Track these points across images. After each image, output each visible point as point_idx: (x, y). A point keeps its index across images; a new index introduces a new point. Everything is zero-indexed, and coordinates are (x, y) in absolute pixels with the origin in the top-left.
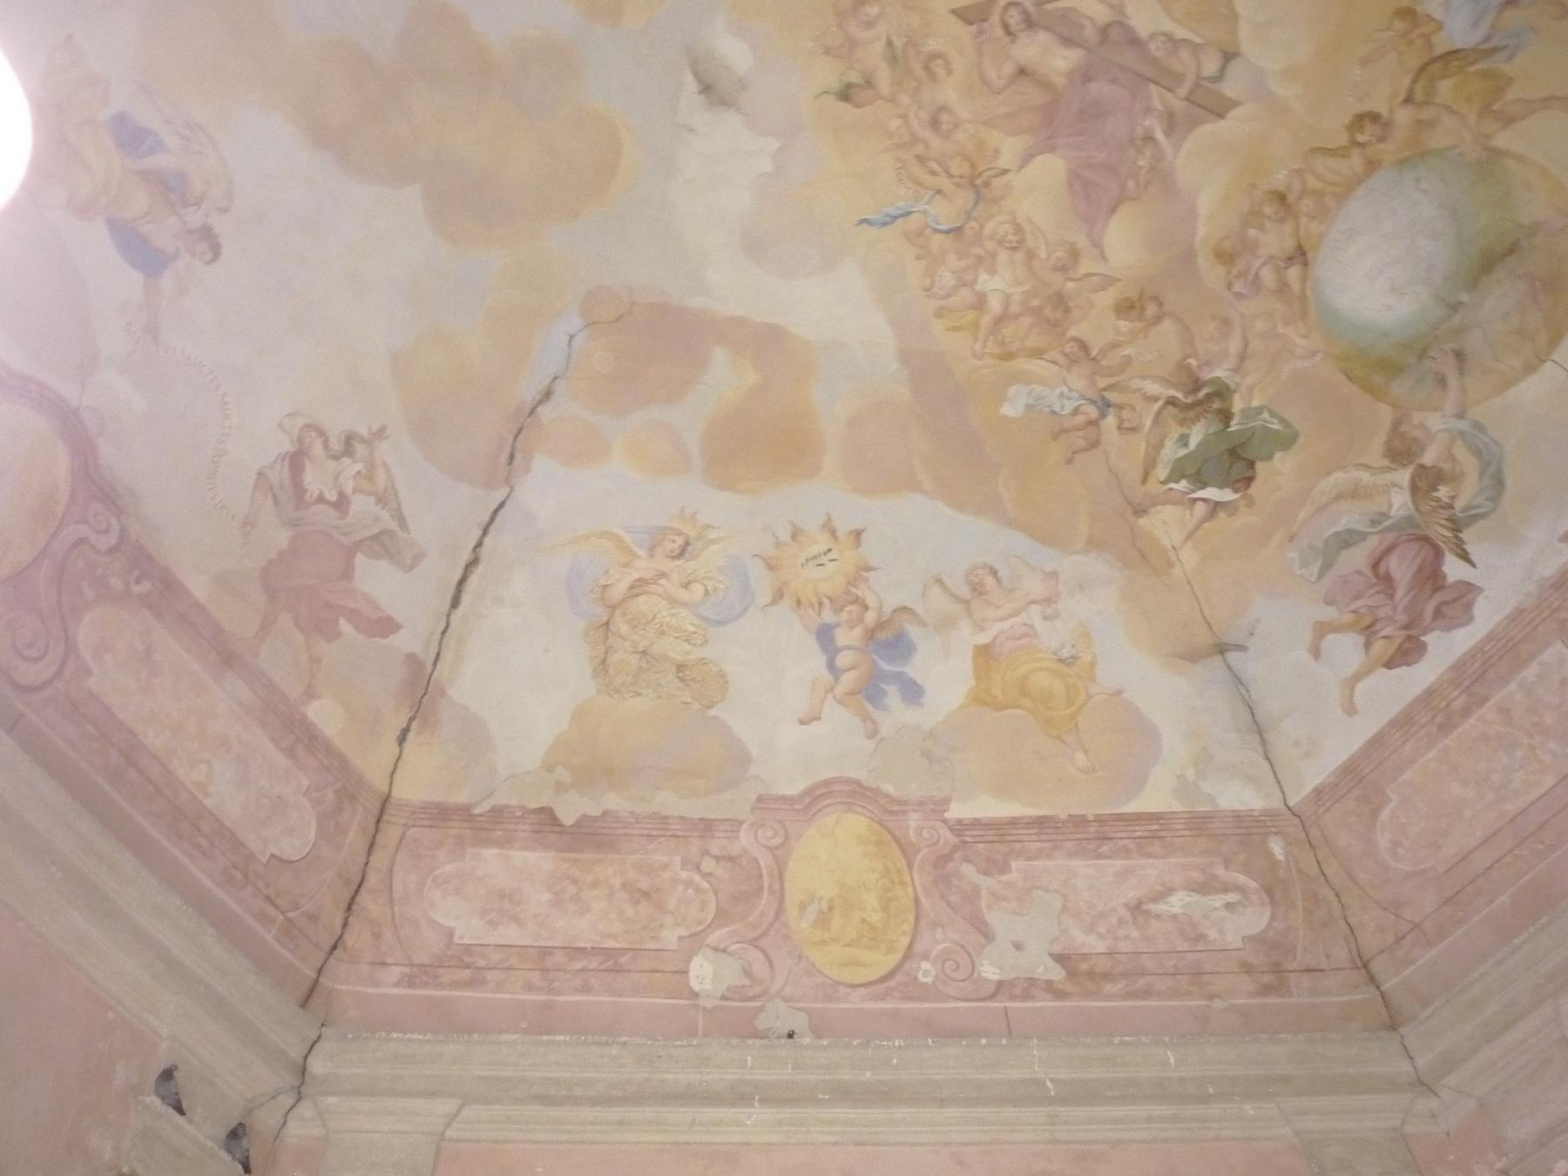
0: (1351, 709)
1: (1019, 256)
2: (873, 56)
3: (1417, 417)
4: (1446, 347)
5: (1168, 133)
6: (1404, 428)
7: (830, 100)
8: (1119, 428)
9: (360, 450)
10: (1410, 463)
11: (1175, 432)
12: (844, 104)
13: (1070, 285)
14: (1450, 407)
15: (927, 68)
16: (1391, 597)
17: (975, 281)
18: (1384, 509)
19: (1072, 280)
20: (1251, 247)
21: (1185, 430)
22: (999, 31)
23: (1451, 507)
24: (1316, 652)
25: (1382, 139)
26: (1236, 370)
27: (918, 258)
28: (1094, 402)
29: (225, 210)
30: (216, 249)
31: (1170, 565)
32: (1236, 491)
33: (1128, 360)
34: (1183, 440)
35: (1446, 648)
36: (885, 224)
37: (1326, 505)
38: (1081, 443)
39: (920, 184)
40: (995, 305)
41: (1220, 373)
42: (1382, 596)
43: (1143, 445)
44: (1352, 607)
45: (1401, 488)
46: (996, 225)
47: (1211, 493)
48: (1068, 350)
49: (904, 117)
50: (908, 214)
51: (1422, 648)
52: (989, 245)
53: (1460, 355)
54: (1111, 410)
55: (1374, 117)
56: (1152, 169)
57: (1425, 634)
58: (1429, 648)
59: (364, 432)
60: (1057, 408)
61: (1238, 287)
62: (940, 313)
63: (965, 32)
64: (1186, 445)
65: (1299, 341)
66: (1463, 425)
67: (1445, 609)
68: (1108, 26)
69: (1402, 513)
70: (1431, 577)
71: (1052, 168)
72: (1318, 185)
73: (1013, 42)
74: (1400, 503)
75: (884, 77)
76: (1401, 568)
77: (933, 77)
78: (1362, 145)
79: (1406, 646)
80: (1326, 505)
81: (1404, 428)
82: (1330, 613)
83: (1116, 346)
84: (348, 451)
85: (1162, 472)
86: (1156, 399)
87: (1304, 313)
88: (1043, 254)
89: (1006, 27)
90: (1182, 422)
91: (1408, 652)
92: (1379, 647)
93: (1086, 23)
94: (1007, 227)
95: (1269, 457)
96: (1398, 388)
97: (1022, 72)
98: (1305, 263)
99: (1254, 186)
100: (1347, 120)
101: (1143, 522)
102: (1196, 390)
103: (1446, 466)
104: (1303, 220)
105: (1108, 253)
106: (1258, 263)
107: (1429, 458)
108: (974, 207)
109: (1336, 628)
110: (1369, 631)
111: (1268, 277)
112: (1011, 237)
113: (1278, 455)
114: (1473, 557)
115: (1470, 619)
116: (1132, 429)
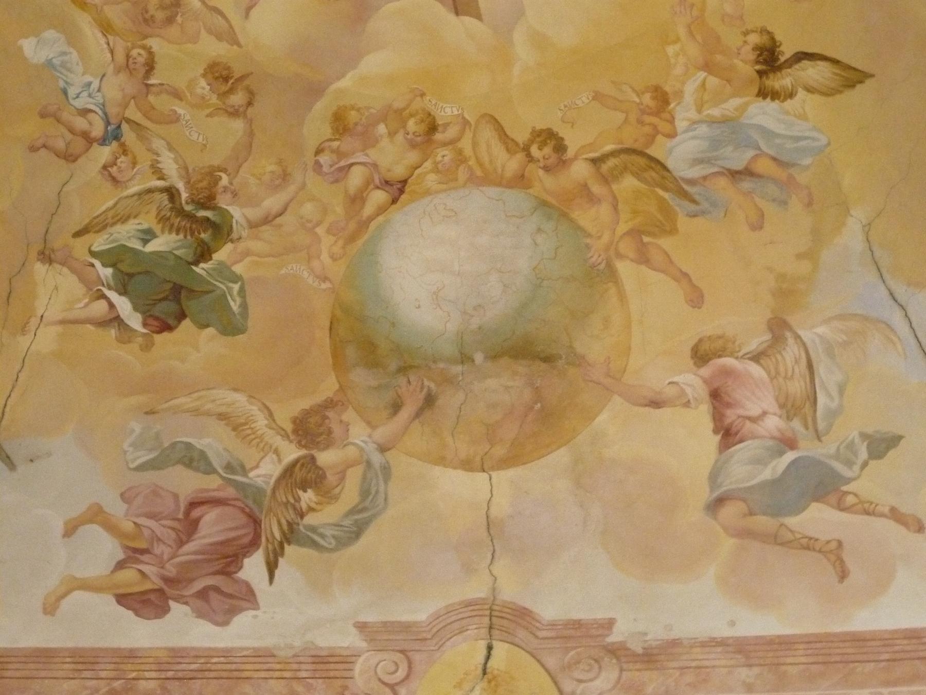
0: (50, 609)
3: (350, 415)
4: (426, 383)
6: (330, 414)
8: (105, 167)
10: (305, 447)
11: (148, 221)
14: (383, 432)
16: (181, 543)
18: (248, 467)
20: (369, 140)
21: (157, 229)
23: (302, 516)
24: (70, 530)
25: (546, 169)
26: (253, 225)
28: (108, 123)
31: (23, 331)
32: (145, 325)
33: (175, 119)
34: (148, 235)
35: (183, 629)
37: (208, 414)
38: (60, 145)
41: (236, 213)
42: (173, 535)
43: (110, 203)
44: (142, 521)
45: (280, 461)
47: (123, 305)
48: (134, 52)
51: (162, 611)
53: (430, 401)
54: (115, 144)
55: (560, 148)
57: (177, 599)
58: (168, 617)
60: (72, 92)
61: (324, 159)
64: (145, 242)
65: (325, 257)
66: (377, 459)
67: (213, 596)
69: (260, 482)
70: (228, 558)
72: (468, 151)
74: (265, 472)
76: (213, 527)
78: (530, 158)
79: (152, 597)
80: (208, 414)
81: (330, 414)
82: (116, 508)
83: (177, 95)
85: (100, 243)
86: (161, 178)
87: (352, 239)
90: (162, 219)
91: (147, 603)
92: (128, 575)
95: (204, 326)
96: (360, 377)
98: (394, 201)
99: (422, 95)
100: (540, 126)
101: (40, 268)
102: (203, 206)
103: (331, 478)
104: (428, 165)
105: (254, 13)
106: (362, 159)
107: (325, 458)
109: (111, 527)
110: (134, 554)
111: (356, 178)
113: (211, 331)
114: (277, 573)
115: (225, 623)
116: (114, 180)
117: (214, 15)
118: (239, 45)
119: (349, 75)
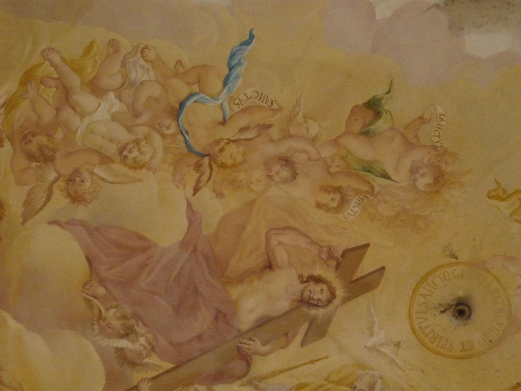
1: (112, 150)
2: (386, 154)
5: (120, 351)
7: (379, 91)
12: (366, 99)
13: (53, 175)
15: (338, 190)
17: (119, 98)
19: (56, 180)
22: (318, 271)
27: (179, 62)
36: (232, 56)
39: (243, 111)
40: (85, 100)
46: (155, 149)
49: (313, 141)
50: (225, 83)
52: (142, 131)
56: (100, 317)
62: (113, 44)
63: (341, 243)
68: (249, 365)
71: (168, 231)
73: (301, 276)
75: (360, 149)
77: (326, 189)
88: (97, 171)
89: (318, 280)
93: (267, 348)
94: (147, 158)
97: (269, 266)
105: (55, 228)
108: (186, 142)
112: (135, 153)
117: (45, 194)
118: (23, 223)
119: (20, 326)
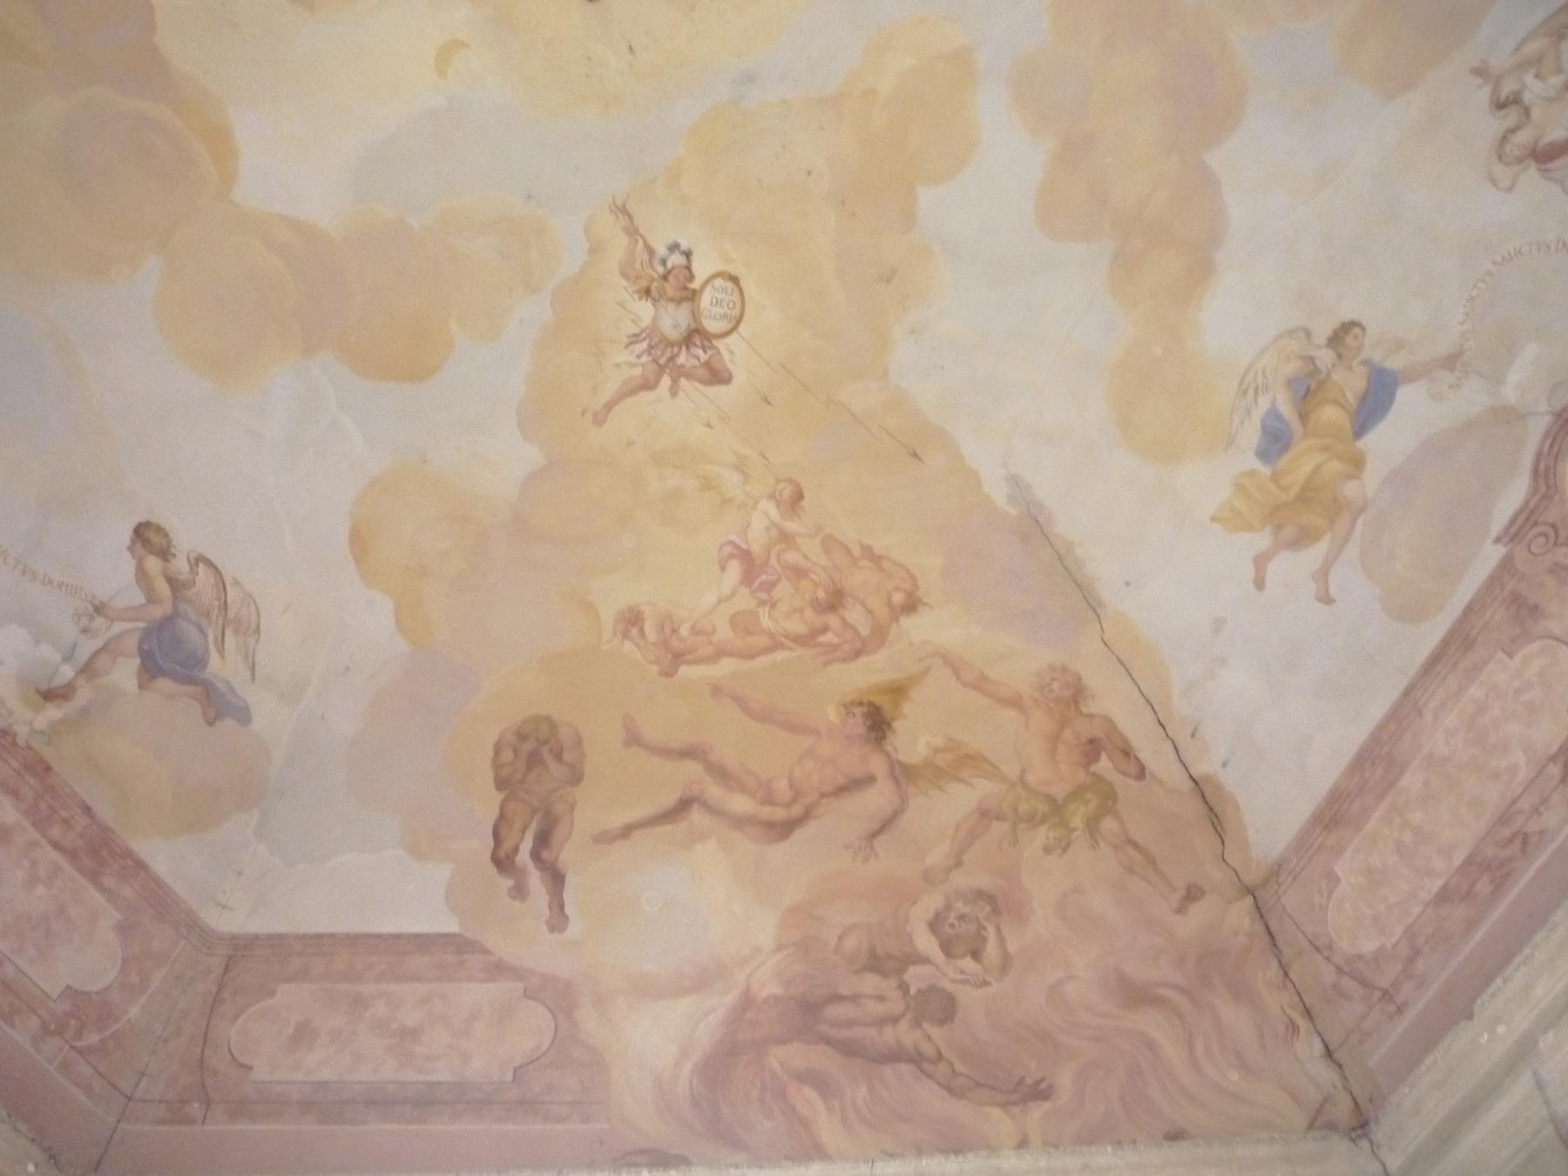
9: (1508, 88)
29: (1308, 334)
30: (1348, 327)
59: (1486, 92)
84: (1515, 100)
